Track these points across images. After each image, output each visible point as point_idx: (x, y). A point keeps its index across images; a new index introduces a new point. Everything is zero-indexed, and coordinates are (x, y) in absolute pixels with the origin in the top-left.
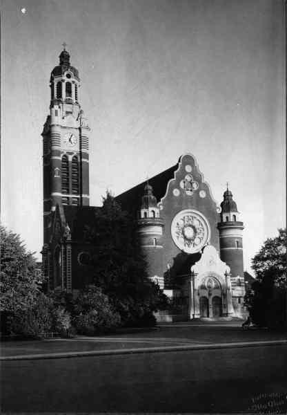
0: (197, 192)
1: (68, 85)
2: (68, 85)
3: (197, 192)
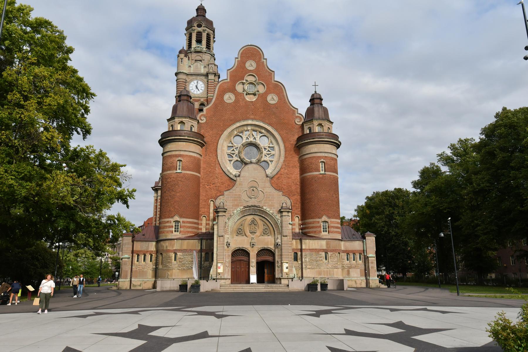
0: (264, 97)
1: (199, 35)
2: (199, 35)
3: (264, 97)
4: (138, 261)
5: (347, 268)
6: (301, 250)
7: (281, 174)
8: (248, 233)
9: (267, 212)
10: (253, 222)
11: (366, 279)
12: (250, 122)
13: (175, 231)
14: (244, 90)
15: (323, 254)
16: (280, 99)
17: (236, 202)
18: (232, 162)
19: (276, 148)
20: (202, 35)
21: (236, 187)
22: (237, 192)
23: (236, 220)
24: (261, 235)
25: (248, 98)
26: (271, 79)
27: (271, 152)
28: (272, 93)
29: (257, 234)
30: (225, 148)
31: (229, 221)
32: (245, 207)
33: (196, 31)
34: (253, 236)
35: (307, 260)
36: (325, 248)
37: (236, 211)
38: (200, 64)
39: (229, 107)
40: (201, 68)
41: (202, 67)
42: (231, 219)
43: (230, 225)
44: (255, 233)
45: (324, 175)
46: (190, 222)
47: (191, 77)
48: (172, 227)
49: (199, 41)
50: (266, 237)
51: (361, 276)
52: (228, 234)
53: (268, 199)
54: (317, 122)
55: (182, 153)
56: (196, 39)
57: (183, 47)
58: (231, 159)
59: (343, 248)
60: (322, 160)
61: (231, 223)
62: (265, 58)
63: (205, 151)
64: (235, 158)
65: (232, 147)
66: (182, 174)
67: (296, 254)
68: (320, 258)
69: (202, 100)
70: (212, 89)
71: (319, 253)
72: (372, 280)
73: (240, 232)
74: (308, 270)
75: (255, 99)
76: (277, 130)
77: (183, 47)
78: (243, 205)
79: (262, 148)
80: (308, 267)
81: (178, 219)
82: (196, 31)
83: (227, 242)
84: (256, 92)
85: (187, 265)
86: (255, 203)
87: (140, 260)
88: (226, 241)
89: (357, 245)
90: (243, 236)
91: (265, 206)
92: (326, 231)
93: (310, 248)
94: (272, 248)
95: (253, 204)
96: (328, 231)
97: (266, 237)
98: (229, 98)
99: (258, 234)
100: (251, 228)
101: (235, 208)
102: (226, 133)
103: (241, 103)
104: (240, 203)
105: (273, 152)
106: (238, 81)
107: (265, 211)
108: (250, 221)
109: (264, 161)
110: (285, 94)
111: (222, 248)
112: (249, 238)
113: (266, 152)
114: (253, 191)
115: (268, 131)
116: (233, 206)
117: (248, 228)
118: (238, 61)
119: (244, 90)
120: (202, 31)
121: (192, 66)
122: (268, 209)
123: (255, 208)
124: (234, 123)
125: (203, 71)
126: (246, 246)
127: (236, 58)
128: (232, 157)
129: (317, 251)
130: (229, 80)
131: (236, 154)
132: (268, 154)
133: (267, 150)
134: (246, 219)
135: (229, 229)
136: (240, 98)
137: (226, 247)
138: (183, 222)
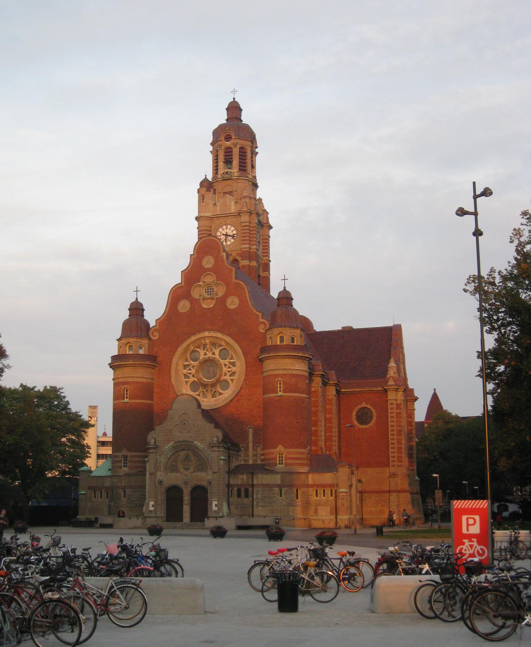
0: (222, 301)
1: (228, 152)
2: (228, 152)
4: (95, 497)
5: (314, 505)
6: (253, 486)
7: (242, 396)
8: (182, 470)
10: (187, 457)
11: (336, 518)
12: (207, 334)
13: (124, 466)
14: (200, 295)
15: (277, 489)
16: (241, 301)
18: (189, 384)
19: (238, 363)
20: (232, 152)
24: (194, 472)
25: (205, 305)
27: (233, 369)
28: (232, 295)
29: (190, 470)
30: (181, 367)
32: (176, 443)
33: (223, 147)
34: (186, 473)
35: (259, 496)
36: (279, 482)
38: (230, 199)
40: (230, 205)
41: (233, 203)
43: (162, 462)
44: (188, 469)
45: (282, 397)
46: (136, 456)
47: (217, 222)
48: (121, 462)
49: (228, 162)
50: (199, 473)
51: (331, 514)
52: (161, 471)
54: (277, 330)
55: (129, 380)
56: (225, 159)
57: (206, 176)
58: (188, 379)
59: (310, 482)
60: (280, 379)
61: (162, 460)
64: (192, 379)
65: (189, 365)
66: (128, 403)
67: (247, 491)
68: (273, 494)
69: (234, 254)
70: (246, 236)
71: (272, 489)
72: (341, 519)
74: (260, 508)
75: (212, 305)
76: (236, 341)
77: (206, 176)
79: (221, 365)
80: (260, 504)
81: (126, 454)
82: (223, 147)
83: (159, 480)
84: (214, 297)
85: (136, 502)
87: (97, 495)
88: (157, 479)
89: (327, 478)
90: (177, 472)
91: (195, 440)
92: (282, 464)
93: (264, 483)
95: (184, 440)
96: (285, 463)
97: (200, 473)
98: (184, 306)
99: (191, 470)
102: (180, 349)
105: (234, 369)
106: (193, 284)
109: (224, 380)
113: (226, 369)
114: (185, 424)
115: (227, 343)
118: (194, 258)
119: (200, 295)
120: (232, 146)
121: (218, 204)
122: (199, 444)
124: (189, 337)
125: (233, 209)
126: (179, 483)
127: (191, 255)
128: (189, 376)
129: (270, 486)
131: (193, 373)
132: (229, 372)
133: (227, 367)
134: (180, 454)
135: (162, 465)
137: (158, 485)
138: (131, 456)
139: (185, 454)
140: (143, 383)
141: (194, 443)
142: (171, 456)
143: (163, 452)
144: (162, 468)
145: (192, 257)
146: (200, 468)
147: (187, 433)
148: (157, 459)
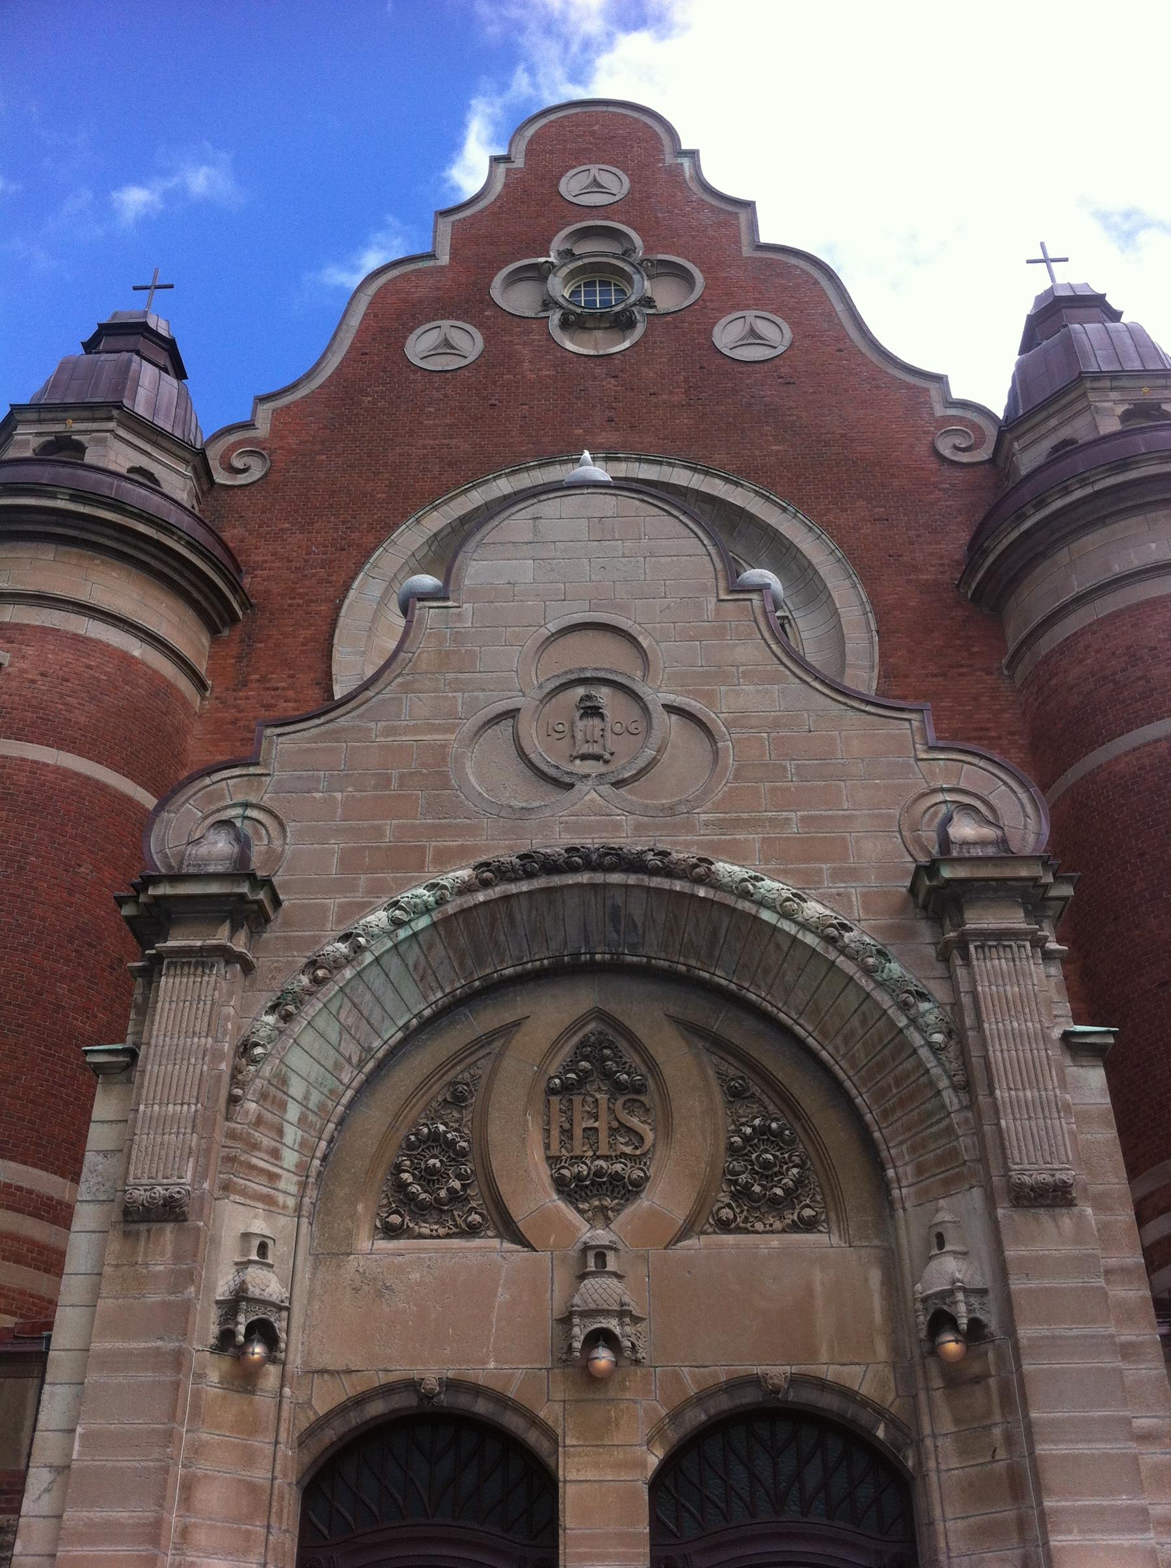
9: (766, 915)
17: (389, 826)
21: (406, 688)
22: (407, 730)
23: (392, 1034)
26: (738, 241)
28: (747, 307)
29: (644, 1202)
31: (297, 1027)
32: (499, 872)
34: (601, 1236)
37: (379, 918)
39: (436, 395)
42: (313, 1007)
43: (297, 1088)
44: (627, 1189)
52: (268, 1200)
53: (764, 787)
54: (1114, 395)
62: (685, 146)
63: (239, 658)
73: (429, 1177)
75: (627, 344)
78: (476, 849)
83: (239, 1299)
84: (634, 309)
86: (617, 827)
88: (223, 1287)
90: (472, 1231)
94: (866, 1389)
95: (591, 841)
97: (775, 1241)
100: (567, 1133)
101: (376, 889)
103: (526, 365)
104: (438, 831)
107: (745, 906)
108: (556, 1045)
110: (839, 307)
111: (147, 1376)
112: (544, 1256)
116: (349, 861)
117: (535, 1137)
119: (548, 303)
123: (615, 878)
130: (444, 259)
134: (517, 1024)
135: (292, 1135)
136: (525, 344)
139: (581, 1022)
140: (126, 658)
141: (709, 879)
142: (411, 1037)
143: (336, 965)
144: (290, 1158)
145: (502, 168)
146: (766, 1172)
147: (618, 784)
148: (245, 1048)
